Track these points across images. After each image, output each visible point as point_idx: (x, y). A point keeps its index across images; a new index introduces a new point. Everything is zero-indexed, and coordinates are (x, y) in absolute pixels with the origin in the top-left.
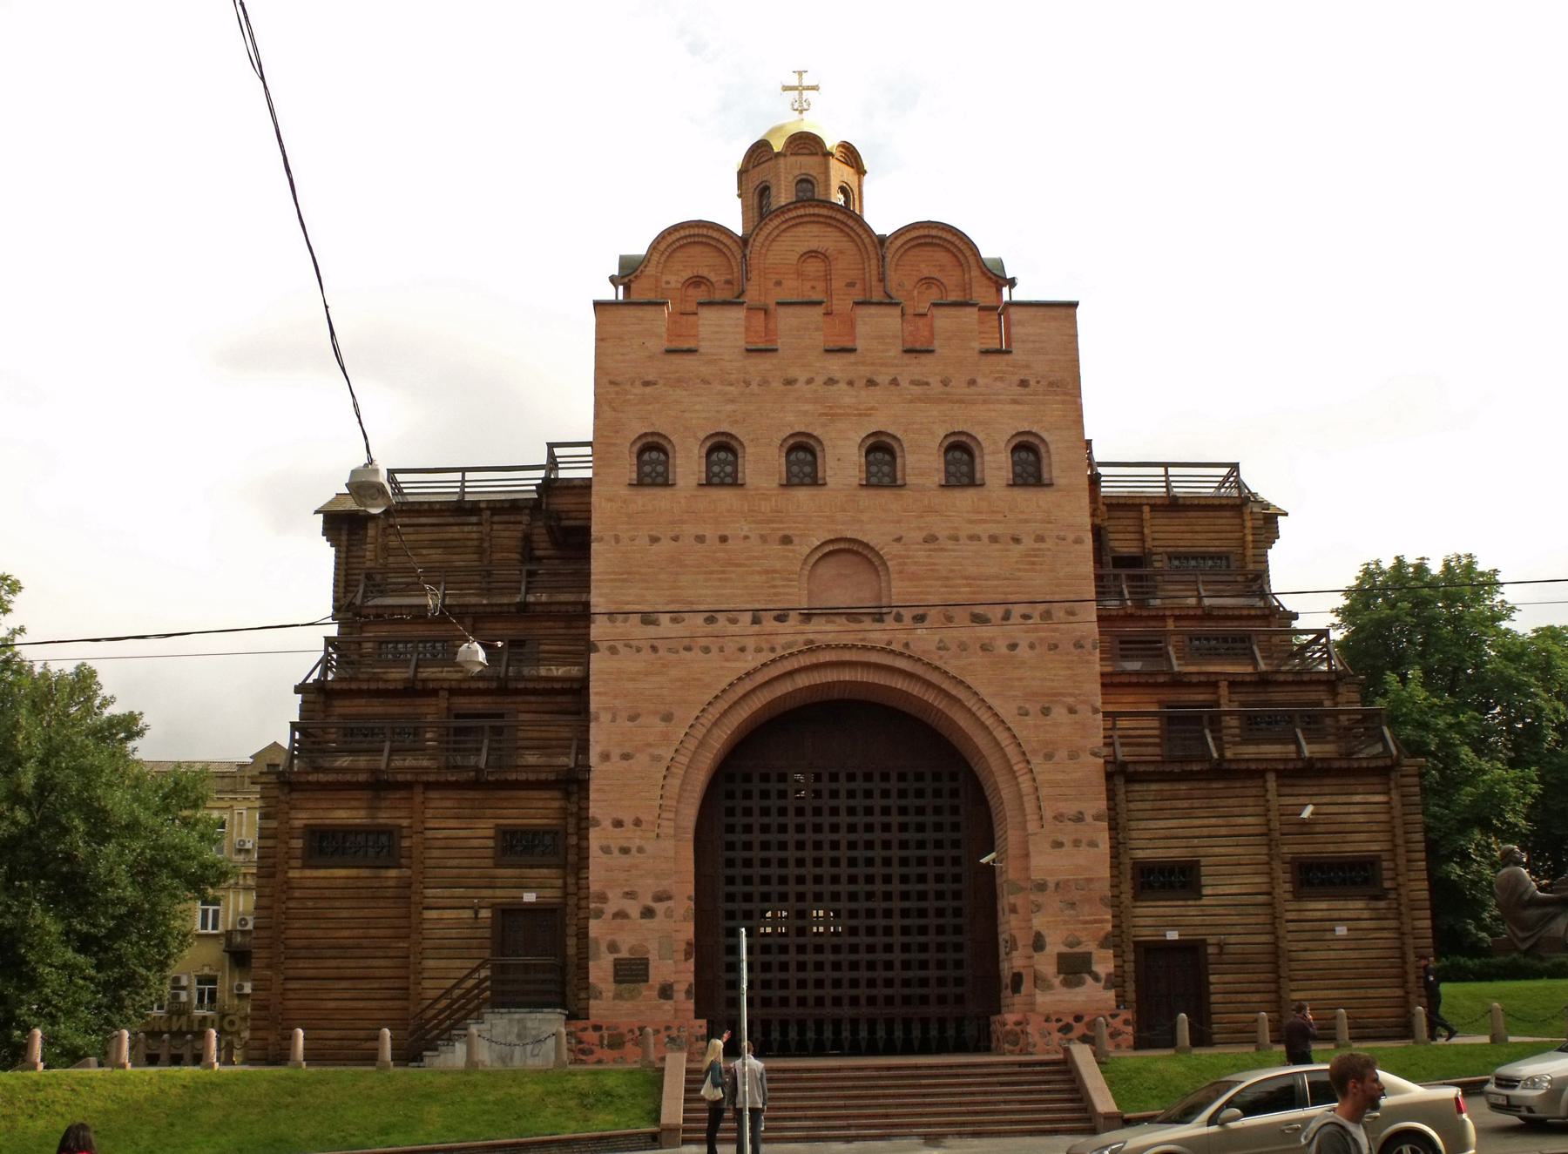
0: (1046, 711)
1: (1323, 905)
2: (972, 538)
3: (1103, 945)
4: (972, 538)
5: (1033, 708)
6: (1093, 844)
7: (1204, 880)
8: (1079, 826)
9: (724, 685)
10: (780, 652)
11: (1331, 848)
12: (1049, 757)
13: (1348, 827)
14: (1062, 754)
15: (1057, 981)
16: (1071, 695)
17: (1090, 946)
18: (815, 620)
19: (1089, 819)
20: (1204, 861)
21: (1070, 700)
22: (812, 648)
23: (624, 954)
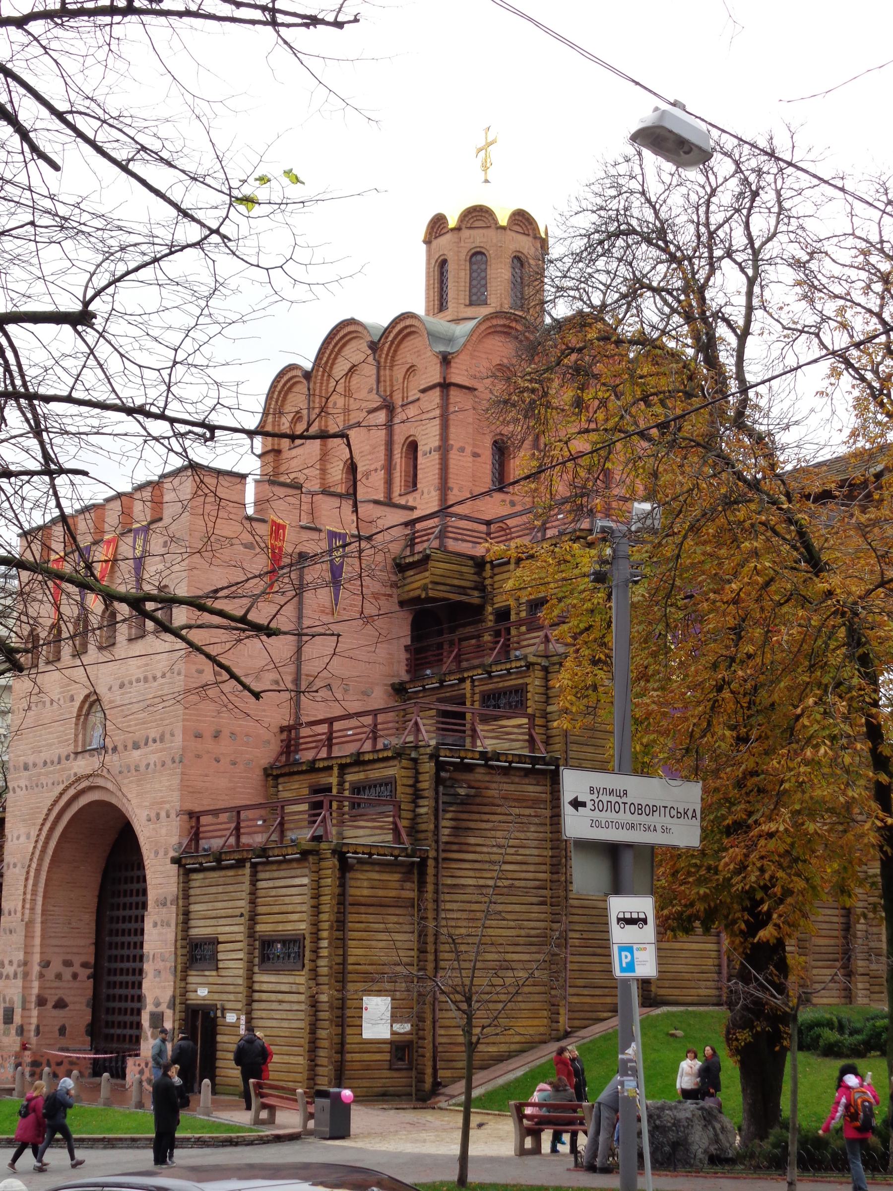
0: (158, 815)
1: (273, 978)
2: (138, 681)
3: (168, 1007)
4: (138, 681)
5: (153, 816)
6: (168, 925)
7: (220, 956)
8: (165, 910)
9: (45, 811)
10: (66, 784)
11: (280, 927)
12: (157, 853)
13: (290, 908)
14: (161, 853)
15: (149, 1034)
16: (168, 802)
17: (163, 1007)
18: (80, 757)
19: (168, 903)
20: (221, 938)
21: (167, 806)
22: (78, 780)
23: (7, 1005)
